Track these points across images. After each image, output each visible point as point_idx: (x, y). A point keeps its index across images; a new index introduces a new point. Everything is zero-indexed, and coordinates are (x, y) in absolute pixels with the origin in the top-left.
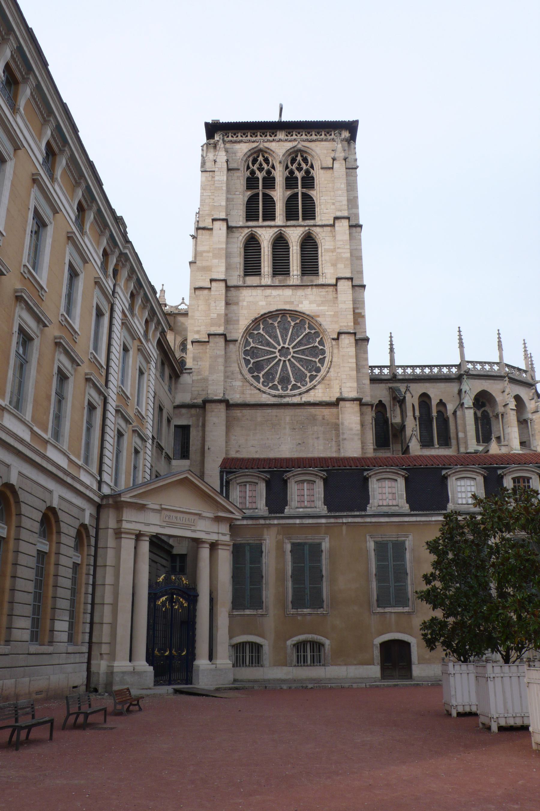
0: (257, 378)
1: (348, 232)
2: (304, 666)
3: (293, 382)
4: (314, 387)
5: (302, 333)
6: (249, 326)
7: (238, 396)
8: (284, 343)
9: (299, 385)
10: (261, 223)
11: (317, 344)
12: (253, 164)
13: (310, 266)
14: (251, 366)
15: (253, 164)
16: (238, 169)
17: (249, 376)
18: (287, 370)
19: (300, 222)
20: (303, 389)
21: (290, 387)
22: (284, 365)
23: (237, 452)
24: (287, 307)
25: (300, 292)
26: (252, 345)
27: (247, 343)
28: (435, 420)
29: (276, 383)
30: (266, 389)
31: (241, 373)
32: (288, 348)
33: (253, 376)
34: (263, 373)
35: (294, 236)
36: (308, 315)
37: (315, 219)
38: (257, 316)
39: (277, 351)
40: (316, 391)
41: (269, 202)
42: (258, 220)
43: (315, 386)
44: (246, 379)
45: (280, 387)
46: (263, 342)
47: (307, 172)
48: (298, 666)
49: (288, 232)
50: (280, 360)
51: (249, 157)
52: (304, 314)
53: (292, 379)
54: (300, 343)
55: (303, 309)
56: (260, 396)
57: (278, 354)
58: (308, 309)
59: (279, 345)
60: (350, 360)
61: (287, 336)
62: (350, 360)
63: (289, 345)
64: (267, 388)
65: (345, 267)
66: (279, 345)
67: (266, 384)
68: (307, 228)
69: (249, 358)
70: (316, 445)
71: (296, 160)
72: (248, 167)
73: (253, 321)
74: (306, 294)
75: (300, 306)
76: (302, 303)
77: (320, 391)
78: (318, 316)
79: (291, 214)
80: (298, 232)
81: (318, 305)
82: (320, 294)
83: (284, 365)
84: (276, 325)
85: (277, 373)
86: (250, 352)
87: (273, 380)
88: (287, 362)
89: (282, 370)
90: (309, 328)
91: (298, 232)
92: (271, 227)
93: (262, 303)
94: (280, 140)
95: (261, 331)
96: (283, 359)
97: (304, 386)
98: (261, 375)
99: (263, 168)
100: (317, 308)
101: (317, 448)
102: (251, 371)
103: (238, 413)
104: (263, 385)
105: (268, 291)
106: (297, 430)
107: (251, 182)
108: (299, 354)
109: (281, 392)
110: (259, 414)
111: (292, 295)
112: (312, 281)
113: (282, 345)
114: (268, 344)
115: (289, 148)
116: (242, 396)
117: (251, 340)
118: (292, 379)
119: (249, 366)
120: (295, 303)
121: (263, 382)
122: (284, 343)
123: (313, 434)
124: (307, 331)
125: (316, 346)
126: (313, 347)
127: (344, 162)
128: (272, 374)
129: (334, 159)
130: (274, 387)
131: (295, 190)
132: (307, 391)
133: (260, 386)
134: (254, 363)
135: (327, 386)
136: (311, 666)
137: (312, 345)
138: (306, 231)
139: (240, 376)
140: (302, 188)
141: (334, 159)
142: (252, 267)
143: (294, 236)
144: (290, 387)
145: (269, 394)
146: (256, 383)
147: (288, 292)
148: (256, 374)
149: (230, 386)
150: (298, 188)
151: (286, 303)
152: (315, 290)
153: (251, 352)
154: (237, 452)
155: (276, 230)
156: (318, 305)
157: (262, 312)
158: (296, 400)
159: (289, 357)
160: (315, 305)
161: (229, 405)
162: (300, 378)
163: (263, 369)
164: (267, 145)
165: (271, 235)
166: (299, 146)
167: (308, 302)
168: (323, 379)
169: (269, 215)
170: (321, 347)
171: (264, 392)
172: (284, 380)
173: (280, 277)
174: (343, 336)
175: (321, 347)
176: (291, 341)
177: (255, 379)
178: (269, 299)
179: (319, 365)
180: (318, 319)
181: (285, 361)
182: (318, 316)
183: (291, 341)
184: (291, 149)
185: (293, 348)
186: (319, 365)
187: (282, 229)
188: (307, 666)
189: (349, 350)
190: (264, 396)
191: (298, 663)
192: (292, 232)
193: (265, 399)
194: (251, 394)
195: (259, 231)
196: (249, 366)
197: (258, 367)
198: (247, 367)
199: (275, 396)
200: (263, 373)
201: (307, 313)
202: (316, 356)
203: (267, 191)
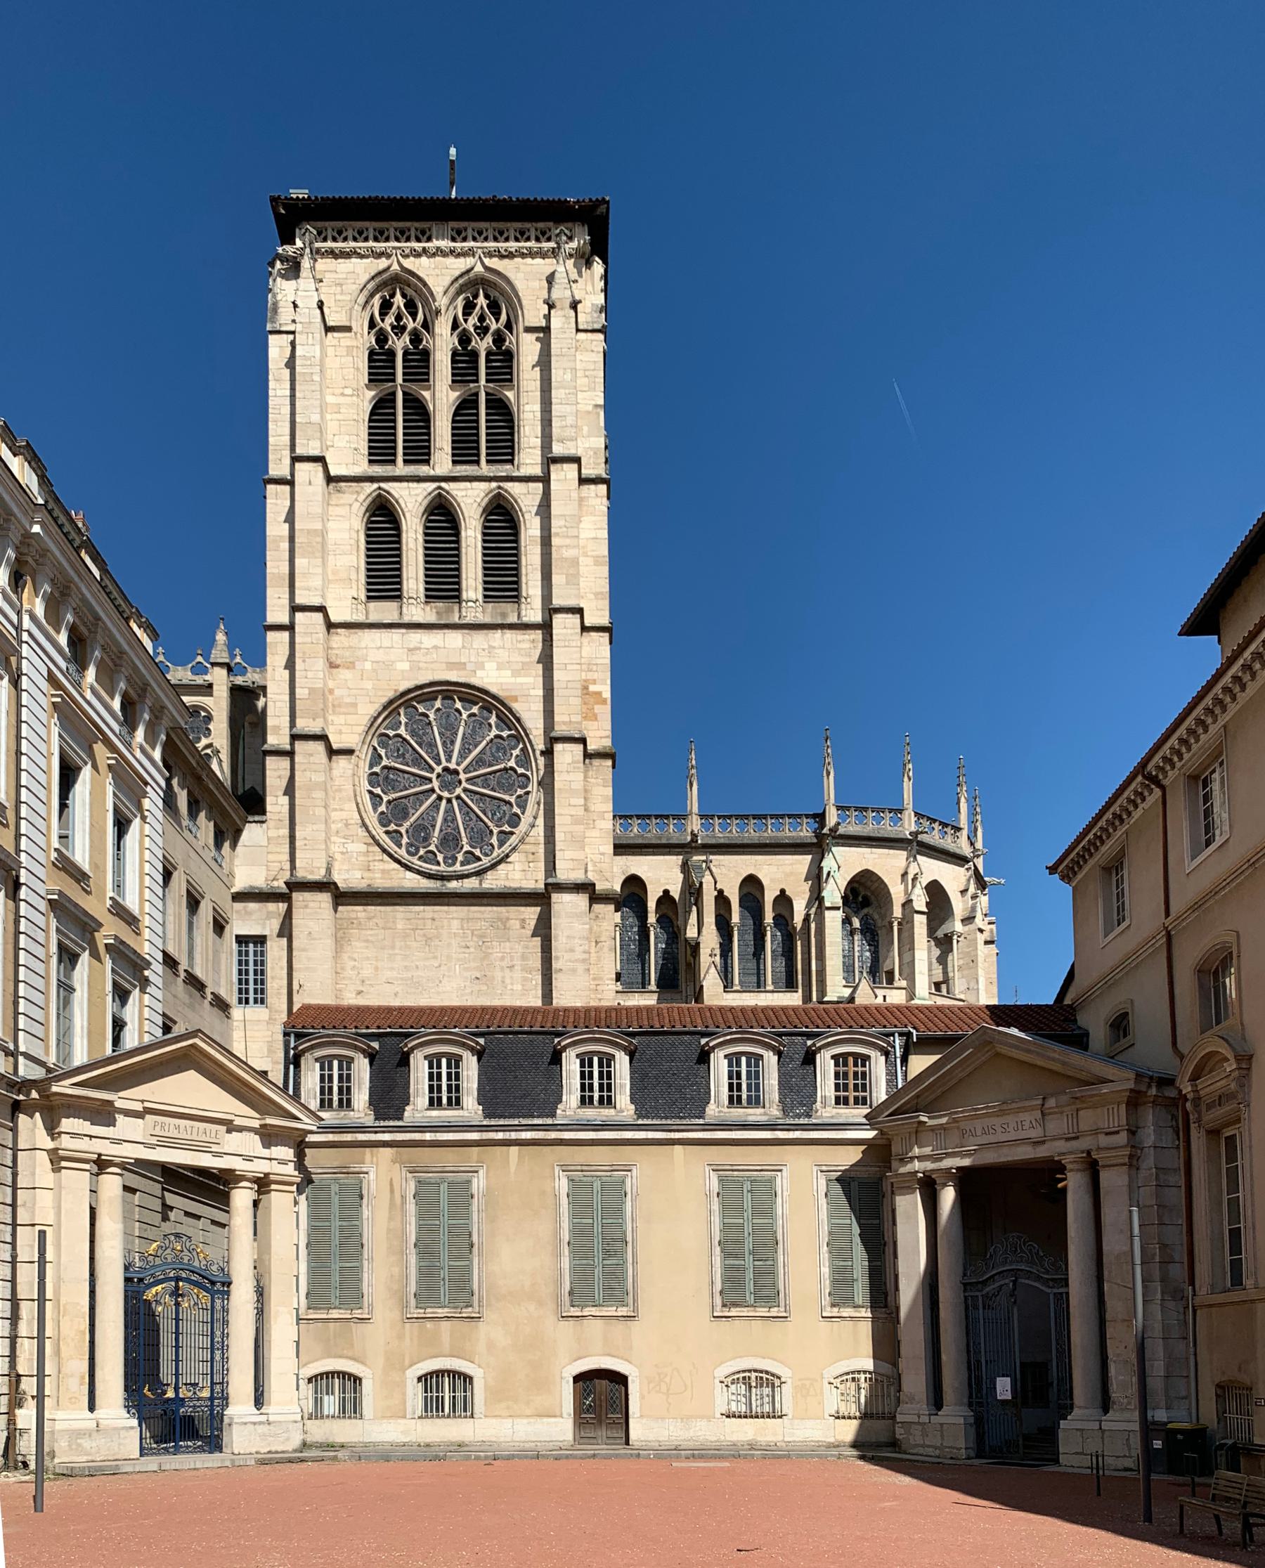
0: (395, 836)
1: (575, 495)
2: (438, 1417)
3: (467, 848)
4: (504, 859)
5: (484, 738)
6: (376, 718)
7: (358, 875)
8: (449, 760)
9: (477, 852)
10: (401, 468)
11: (512, 763)
12: (383, 314)
13: (503, 580)
14: (383, 808)
15: (383, 314)
16: (348, 329)
17: (379, 832)
18: (454, 819)
19: (485, 469)
20: (486, 861)
21: (460, 857)
22: (449, 811)
23: (360, 993)
24: (453, 676)
25: (479, 638)
26: (385, 762)
27: (376, 758)
28: (736, 933)
29: (432, 848)
30: (415, 861)
31: (364, 825)
32: (456, 772)
33: (387, 832)
34: (407, 824)
35: (470, 500)
36: (494, 697)
37: (511, 462)
38: (391, 695)
39: (434, 776)
40: (510, 867)
41: (419, 413)
42: (393, 462)
43: (507, 856)
44: (373, 837)
45: (440, 858)
46: (407, 756)
47: (499, 339)
48: (427, 1417)
49: (454, 493)
50: (440, 798)
51: (372, 295)
52: (486, 692)
53: (465, 840)
54: (479, 762)
55: (486, 680)
56: (401, 875)
57: (436, 784)
58: (494, 680)
59: (439, 763)
60: (573, 801)
61: (453, 742)
62: (573, 801)
63: (458, 764)
64: (415, 860)
65: (567, 583)
66: (439, 763)
67: (413, 849)
68: (494, 485)
69: (378, 791)
70: (508, 981)
71: (476, 305)
72: (372, 324)
73: (385, 708)
74: (491, 647)
75: (479, 673)
76: (481, 666)
77: (518, 866)
78: (515, 699)
79: (464, 450)
80: (476, 492)
81: (516, 673)
82: (519, 646)
83: (449, 811)
84: (432, 717)
85: (434, 826)
86: (381, 779)
87: (426, 839)
88: (455, 803)
89: (445, 820)
90: (497, 728)
91: (476, 492)
92: (419, 479)
93: (405, 666)
94: (440, 252)
95: (402, 731)
96: (446, 794)
97: (486, 855)
98: (403, 830)
99: (404, 328)
100: (513, 680)
101: (509, 987)
102: (384, 820)
103: (358, 912)
104: (408, 852)
105: (416, 637)
106: (472, 950)
107: (380, 363)
108: (477, 785)
109: (442, 868)
110: (400, 914)
111: (464, 647)
112: (504, 615)
113: (444, 764)
114: (418, 761)
115: (457, 273)
116: (366, 875)
117: (382, 752)
118: (465, 840)
119: (380, 810)
120: (470, 667)
121: (410, 845)
122: (449, 760)
123: (502, 959)
124: (494, 732)
125: (512, 769)
126: (505, 769)
127: (572, 313)
128: (425, 828)
129: (551, 306)
130: (430, 858)
131: (472, 385)
132: (493, 866)
133: (402, 852)
134: (389, 802)
135: (531, 857)
136: (449, 1416)
137: (502, 766)
138: (491, 491)
139: (362, 832)
140: (488, 381)
141: (551, 306)
142: (383, 580)
143: (470, 500)
144: (460, 857)
145: (419, 872)
146: (392, 847)
147: (455, 639)
148: (392, 827)
149: (342, 853)
150: (477, 381)
151: (452, 666)
152: (509, 634)
153: (381, 779)
154: (360, 993)
155: (431, 486)
156: (516, 673)
157: (402, 688)
158: (470, 884)
159: (459, 791)
160: (509, 673)
161: (342, 897)
162: (480, 836)
163: (406, 816)
164: (409, 263)
165: (420, 499)
166: (479, 268)
167: (494, 665)
168: (522, 841)
169: (420, 452)
170: (520, 771)
171: (408, 868)
172: (450, 841)
173: (440, 605)
174: (558, 747)
175: (520, 771)
176: (462, 756)
177: (392, 839)
178: (417, 656)
179: (516, 810)
180: (515, 706)
181: (449, 801)
182: (515, 699)
183: (462, 756)
184: (461, 275)
185: (466, 771)
186: (516, 810)
187: (443, 485)
188: (443, 1416)
189: (572, 777)
190: (409, 875)
191: (426, 1411)
192: (464, 493)
193: (411, 882)
194: (383, 871)
195: (397, 490)
196: (380, 810)
197: (398, 811)
198: (375, 809)
199: (429, 876)
200: (407, 824)
201: (494, 690)
202: (509, 789)
203: (413, 387)
